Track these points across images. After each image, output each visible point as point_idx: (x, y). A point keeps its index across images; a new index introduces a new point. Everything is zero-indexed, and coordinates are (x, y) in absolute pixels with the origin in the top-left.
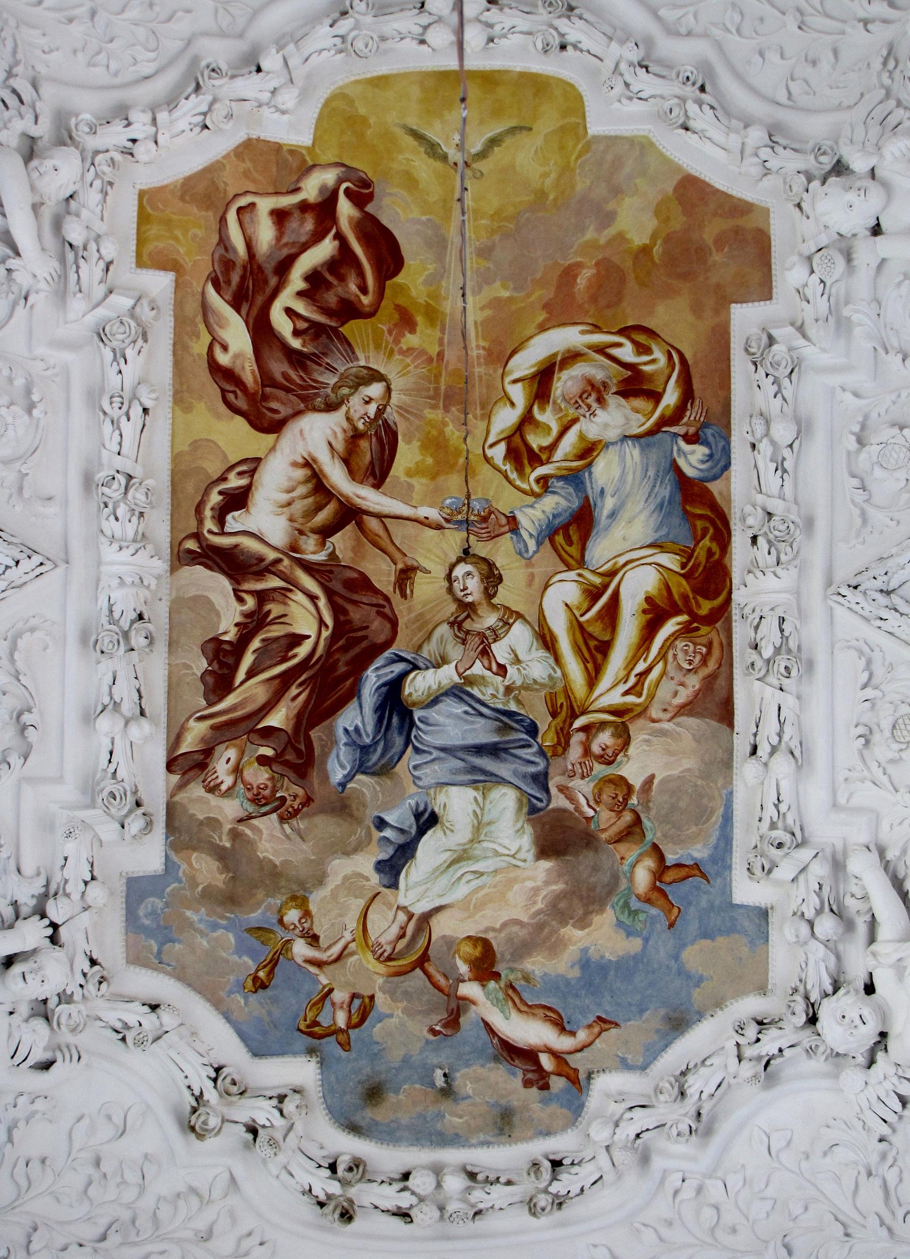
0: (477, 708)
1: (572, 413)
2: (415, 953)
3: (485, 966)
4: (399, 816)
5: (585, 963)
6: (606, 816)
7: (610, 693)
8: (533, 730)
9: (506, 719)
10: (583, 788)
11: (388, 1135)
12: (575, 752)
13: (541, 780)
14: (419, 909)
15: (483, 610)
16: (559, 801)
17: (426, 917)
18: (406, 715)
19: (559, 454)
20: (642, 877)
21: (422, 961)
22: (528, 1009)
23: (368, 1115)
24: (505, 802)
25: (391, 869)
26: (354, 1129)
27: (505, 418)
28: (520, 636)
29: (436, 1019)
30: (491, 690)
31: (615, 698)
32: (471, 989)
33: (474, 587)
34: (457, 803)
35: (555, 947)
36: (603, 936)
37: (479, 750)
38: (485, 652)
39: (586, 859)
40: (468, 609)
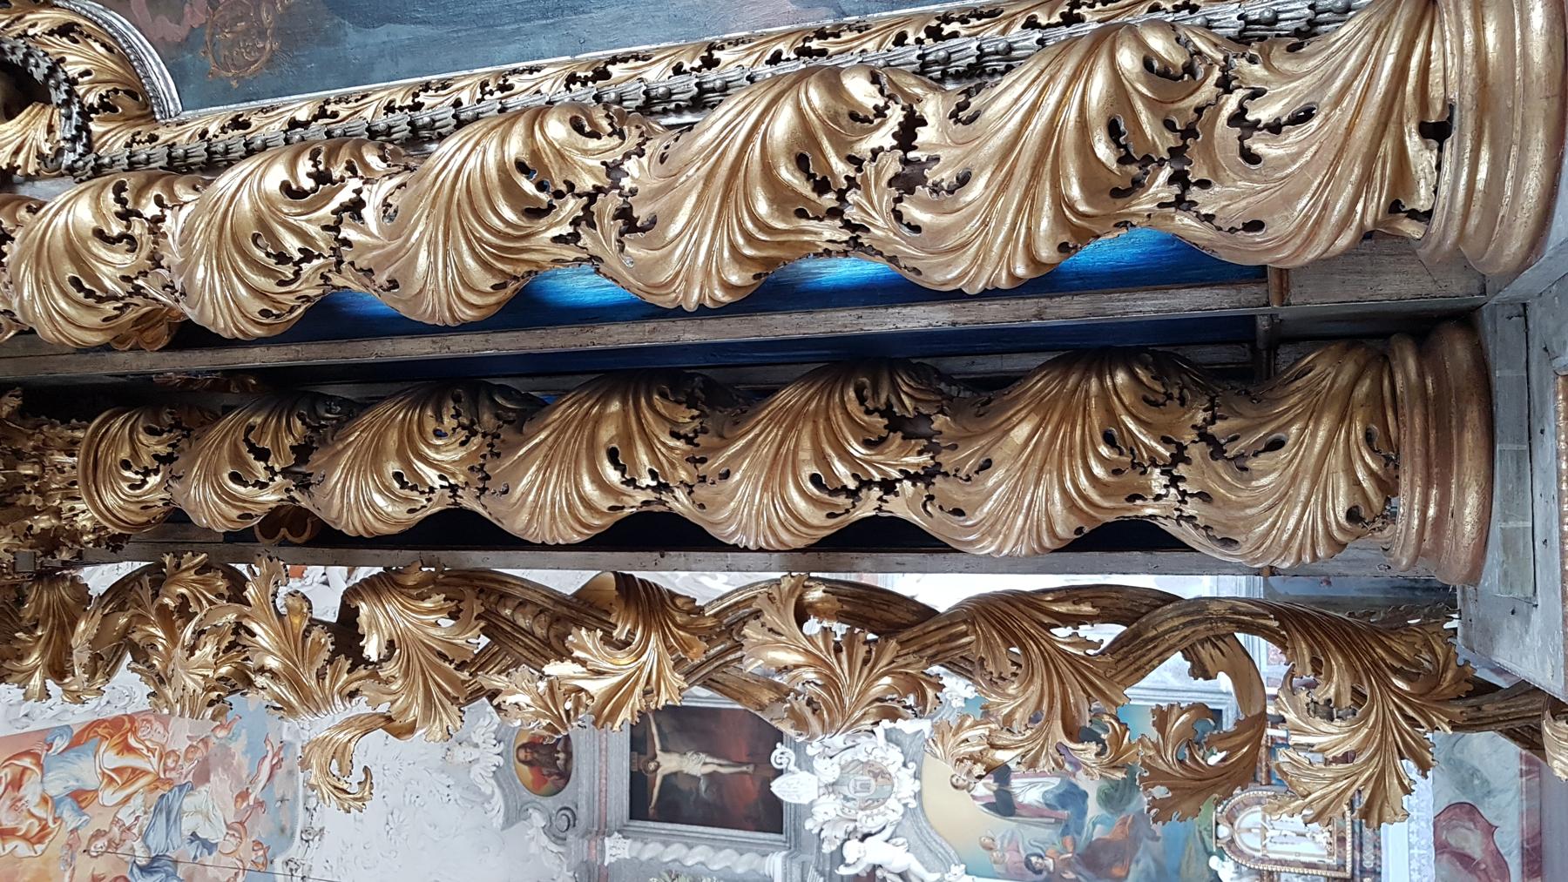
0: (151, 826)
1: (25, 813)
2: (238, 828)
3: (244, 795)
4: (192, 850)
5: (245, 753)
6: (199, 755)
7: (152, 764)
8: (162, 796)
9: (158, 811)
10: (187, 767)
11: (294, 820)
12: (172, 775)
13: (181, 787)
14: (225, 831)
15: (110, 835)
16: (190, 778)
17: (228, 827)
18: (154, 859)
19: (44, 815)
20: (221, 733)
21: (242, 823)
22: (257, 775)
23: (288, 832)
24: (189, 803)
25: (209, 846)
26: (293, 835)
27: (23, 849)
28: (125, 815)
29: (260, 810)
30: (144, 821)
31: (155, 761)
32: (252, 798)
33: (101, 843)
34: (187, 824)
35: (240, 765)
36: (237, 747)
37: (168, 820)
38: (129, 829)
39: (211, 760)
40: (110, 841)
